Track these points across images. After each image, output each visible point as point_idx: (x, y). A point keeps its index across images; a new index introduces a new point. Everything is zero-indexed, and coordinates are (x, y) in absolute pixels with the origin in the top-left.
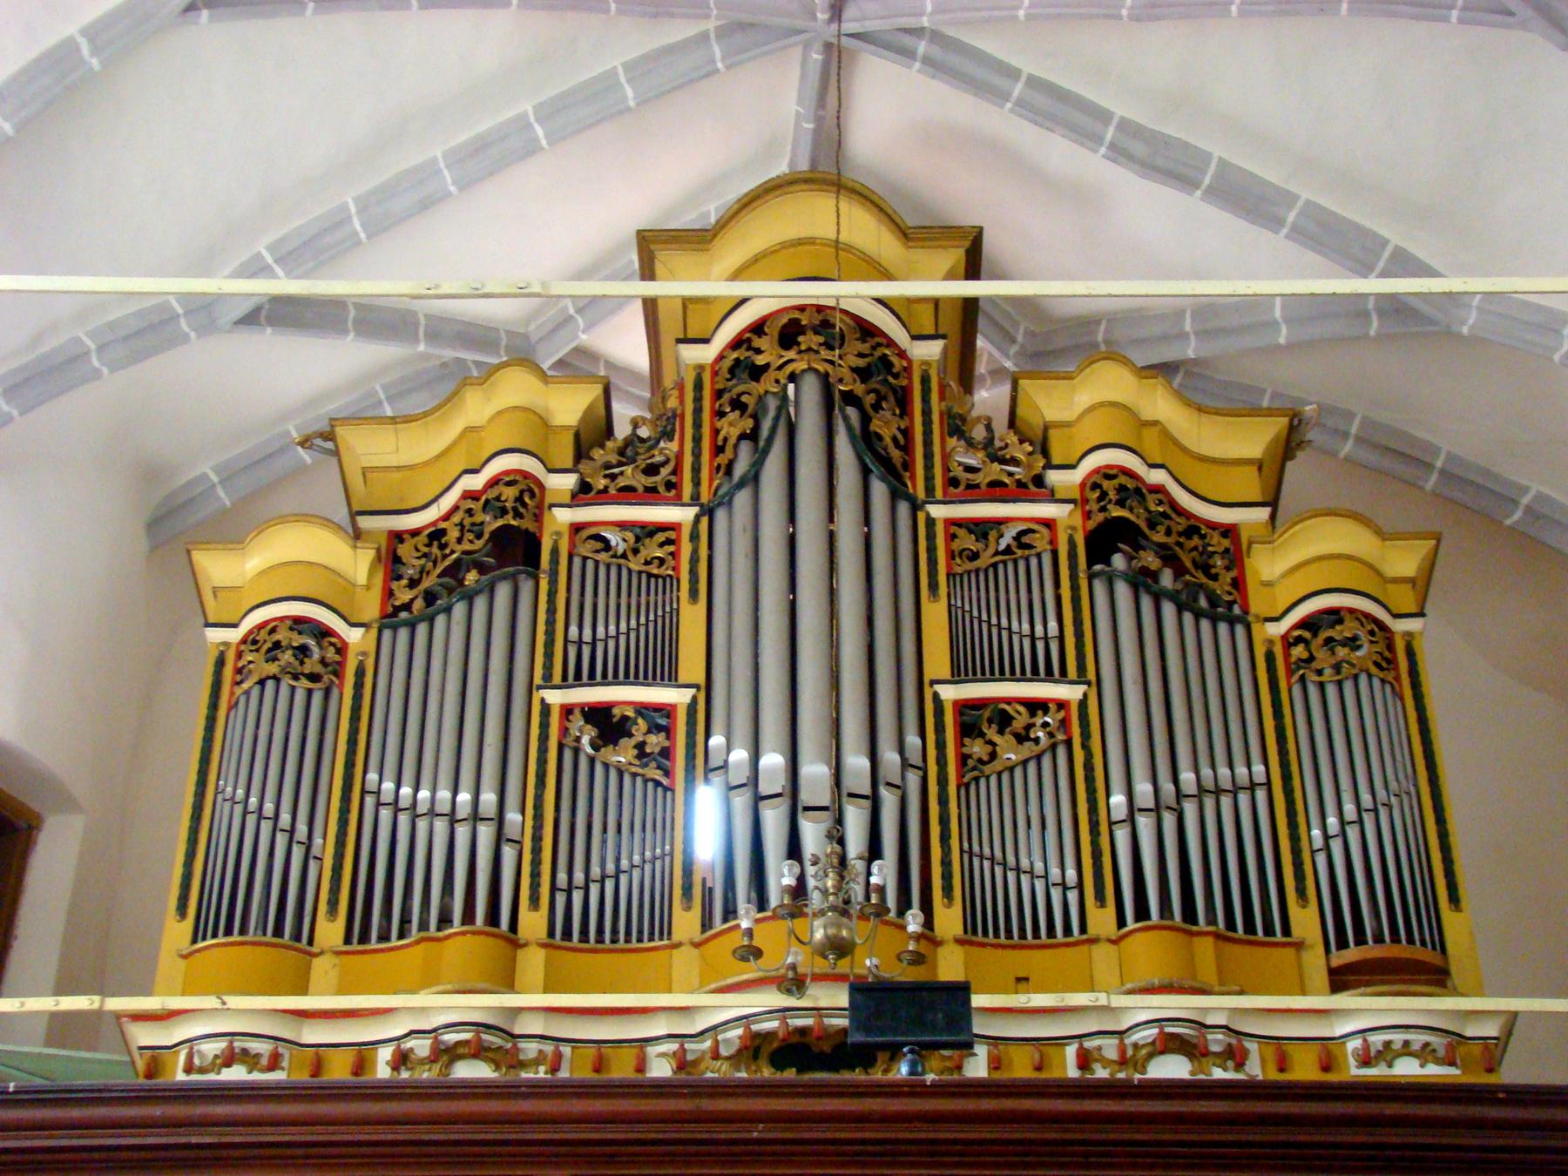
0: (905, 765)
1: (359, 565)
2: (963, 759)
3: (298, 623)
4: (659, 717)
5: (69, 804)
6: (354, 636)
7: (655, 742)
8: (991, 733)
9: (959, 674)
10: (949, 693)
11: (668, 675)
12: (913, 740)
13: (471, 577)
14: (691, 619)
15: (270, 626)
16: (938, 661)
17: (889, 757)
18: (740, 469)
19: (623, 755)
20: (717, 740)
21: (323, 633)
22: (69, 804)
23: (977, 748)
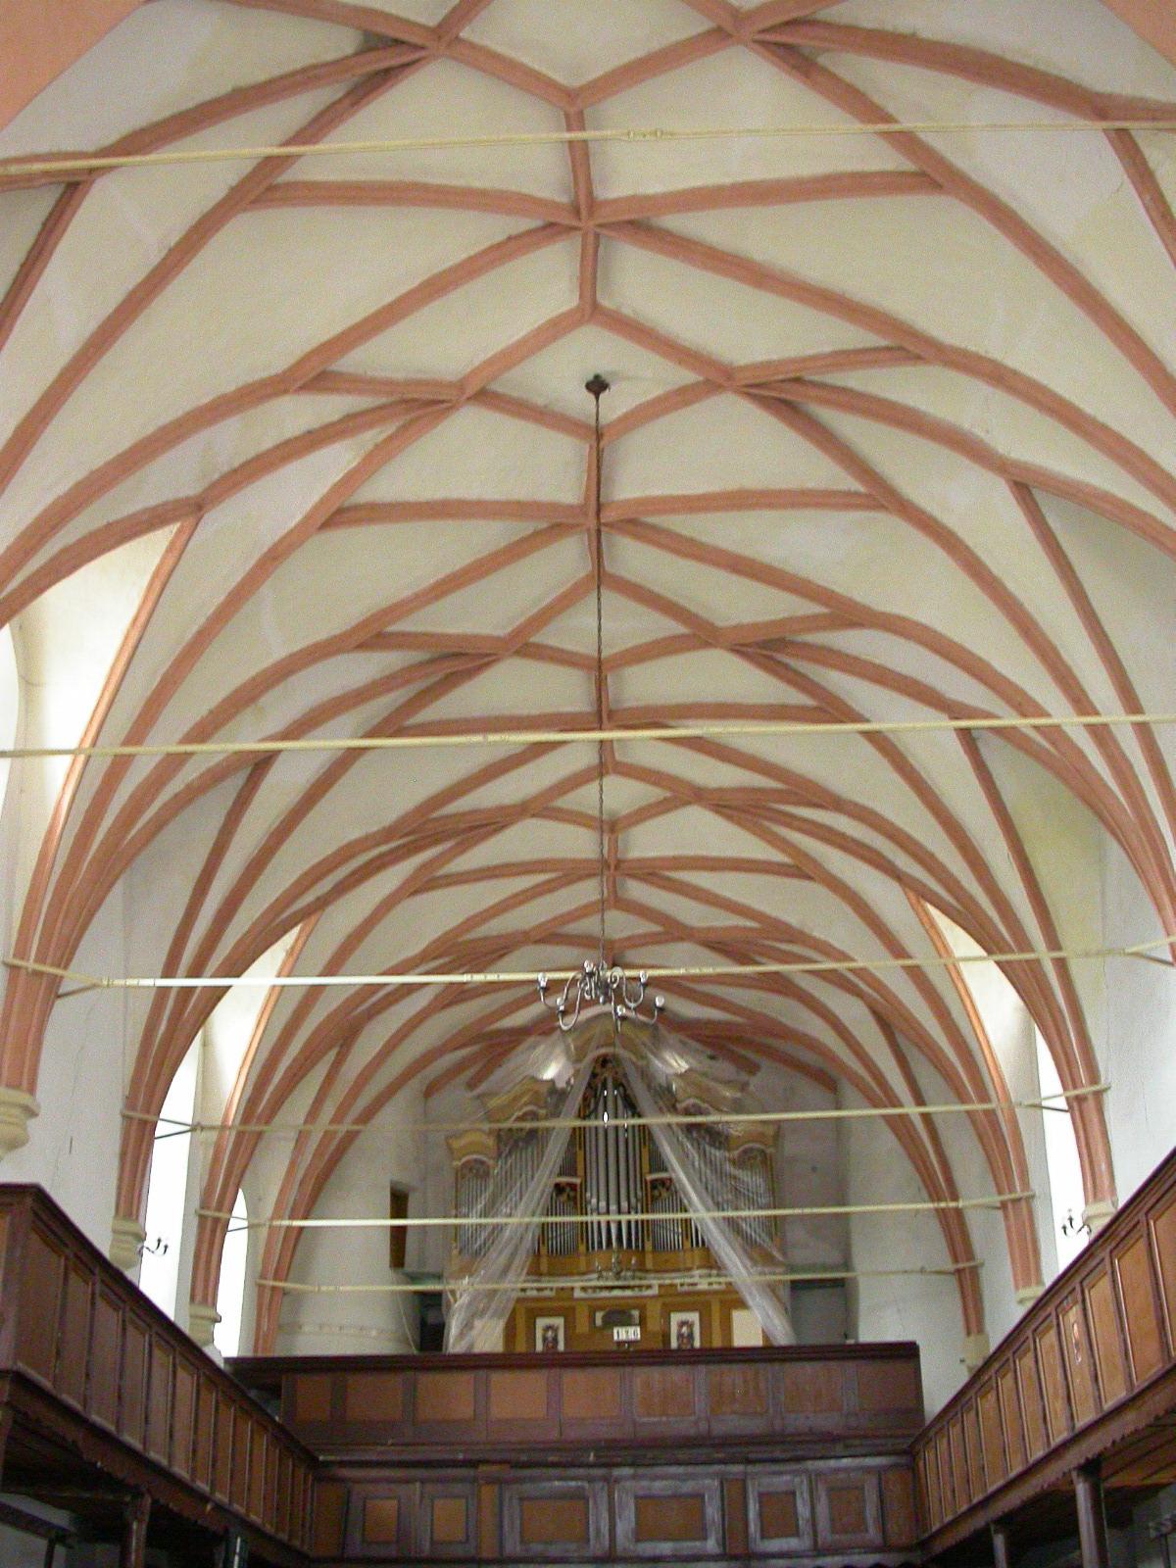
0: (637, 1200)
1: (491, 1142)
2: (652, 1197)
3: (476, 1161)
4: (573, 1187)
5: (414, 1189)
6: (491, 1162)
7: (572, 1194)
8: (660, 1188)
9: (651, 1172)
10: (649, 1177)
11: (575, 1174)
12: (639, 1193)
13: (521, 1144)
14: (580, 1154)
15: (468, 1162)
16: (646, 1167)
17: (633, 1200)
18: (592, 1106)
19: (563, 1198)
20: (588, 1195)
21: (482, 1163)
22: (414, 1189)
23: (656, 1193)
